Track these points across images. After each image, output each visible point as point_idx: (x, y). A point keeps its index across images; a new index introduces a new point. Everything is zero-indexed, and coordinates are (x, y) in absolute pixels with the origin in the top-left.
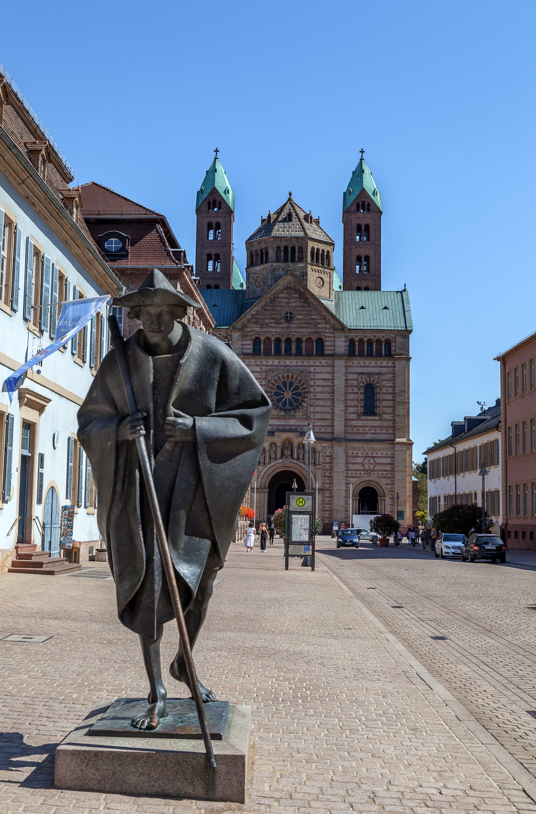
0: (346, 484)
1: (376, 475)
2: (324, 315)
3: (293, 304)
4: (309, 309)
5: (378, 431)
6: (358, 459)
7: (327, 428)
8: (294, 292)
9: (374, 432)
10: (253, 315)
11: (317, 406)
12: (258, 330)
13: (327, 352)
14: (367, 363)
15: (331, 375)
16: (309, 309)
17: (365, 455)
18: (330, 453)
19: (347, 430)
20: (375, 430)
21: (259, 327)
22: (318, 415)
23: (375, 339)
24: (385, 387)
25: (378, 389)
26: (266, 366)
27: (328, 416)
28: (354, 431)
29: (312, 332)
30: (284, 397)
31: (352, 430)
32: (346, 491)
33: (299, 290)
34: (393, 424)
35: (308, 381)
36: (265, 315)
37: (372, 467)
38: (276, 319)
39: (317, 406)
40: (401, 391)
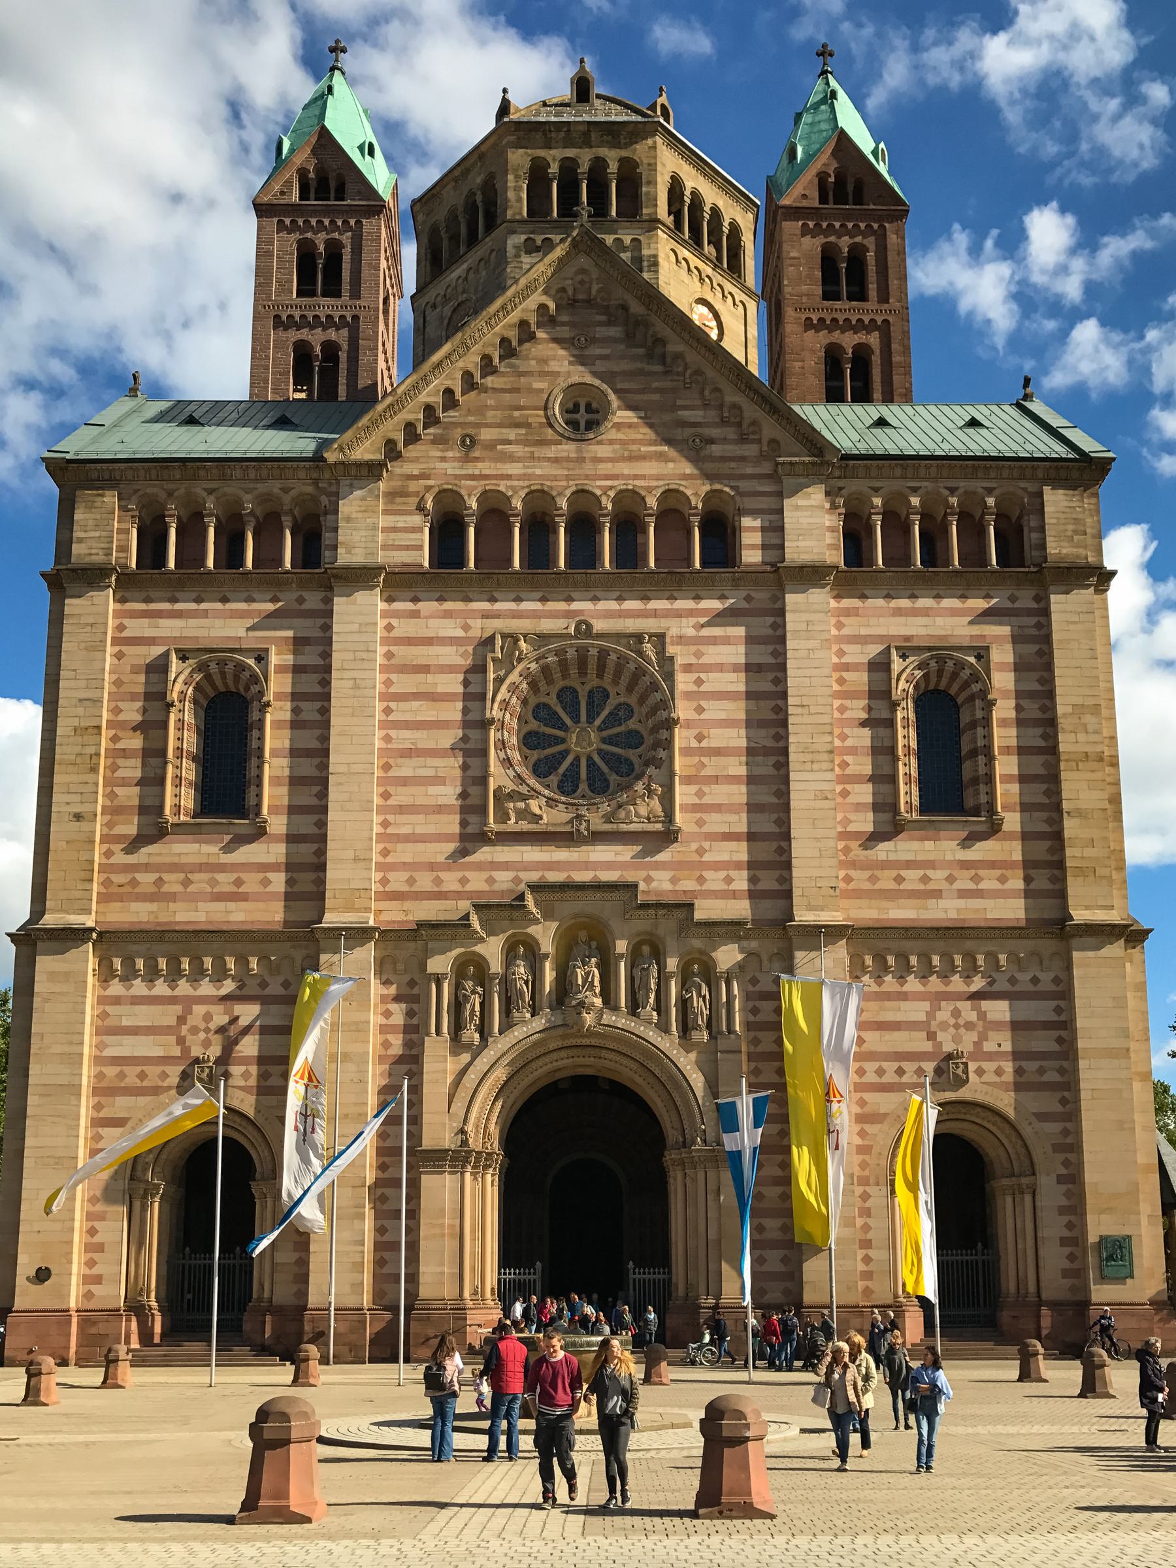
1: (990, 1077)
2: (735, 407)
4: (667, 384)
6: (904, 1005)
8: (603, 318)
9: (972, 886)
11: (716, 779)
12: (452, 468)
15: (770, 648)
16: (667, 384)
20: (976, 879)
21: (454, 459)
22: (715, 817)
25: (978, 703)
26: (486, 615)
28: (877, 886)
29: (685, 477)
30: (566, 752)
31: (873, 879)
33: (624, 308)
34: (1051, 850)
35: (669, 677)
36: (482, 410)
38: (528, 425)
39: (716, 779)
40: (1079, 709)
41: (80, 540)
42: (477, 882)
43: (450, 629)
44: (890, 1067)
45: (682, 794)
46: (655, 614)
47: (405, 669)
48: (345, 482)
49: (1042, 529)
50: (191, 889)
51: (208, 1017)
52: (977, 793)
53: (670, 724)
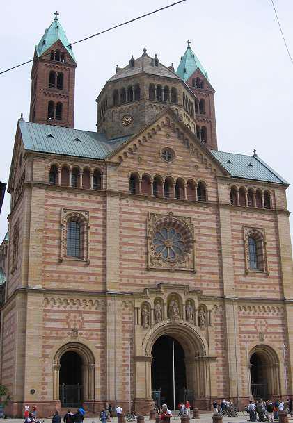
0: (241, 349)
2: (206, 160)
3: (172, 144)
5: (266, 289)
6: (250, 319)
7: (216, 284)
9: (262, 289)
10: (130, 149)
11: (204, 258)
12: (136, 166)
13: (209, 199)
14: (250, 215)
17: (256, 315)
18: (221, 313)
19: (235, 286)
20: (264, 287)
21: (137, 164)
23: (255, 189)
24: (270, 241)
27: (216, 270)
31: (241, 286)
32: (242, 357)
35: (193, 229)
37: (264, 328)
39: (204, 258)
41: (35, 174)
42: (145, 282)
43: (137, 210)
44: (247, 335)
45: (197, 261)
46: (187, 211)
47: (124, 220)
48: (108, 167)
49: (275, 200)
50: (69, 279)
51: (75, 317)
52: (263, 266)
53: (194, 242)
